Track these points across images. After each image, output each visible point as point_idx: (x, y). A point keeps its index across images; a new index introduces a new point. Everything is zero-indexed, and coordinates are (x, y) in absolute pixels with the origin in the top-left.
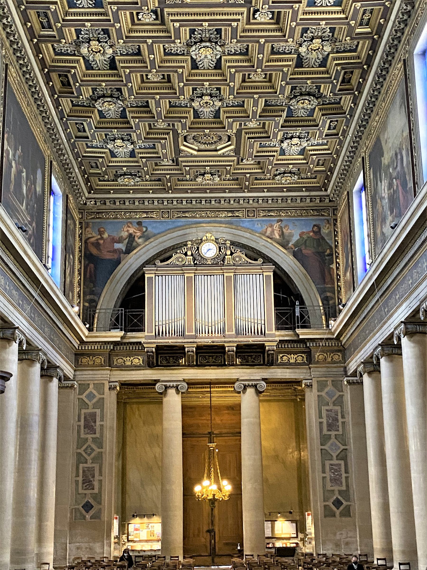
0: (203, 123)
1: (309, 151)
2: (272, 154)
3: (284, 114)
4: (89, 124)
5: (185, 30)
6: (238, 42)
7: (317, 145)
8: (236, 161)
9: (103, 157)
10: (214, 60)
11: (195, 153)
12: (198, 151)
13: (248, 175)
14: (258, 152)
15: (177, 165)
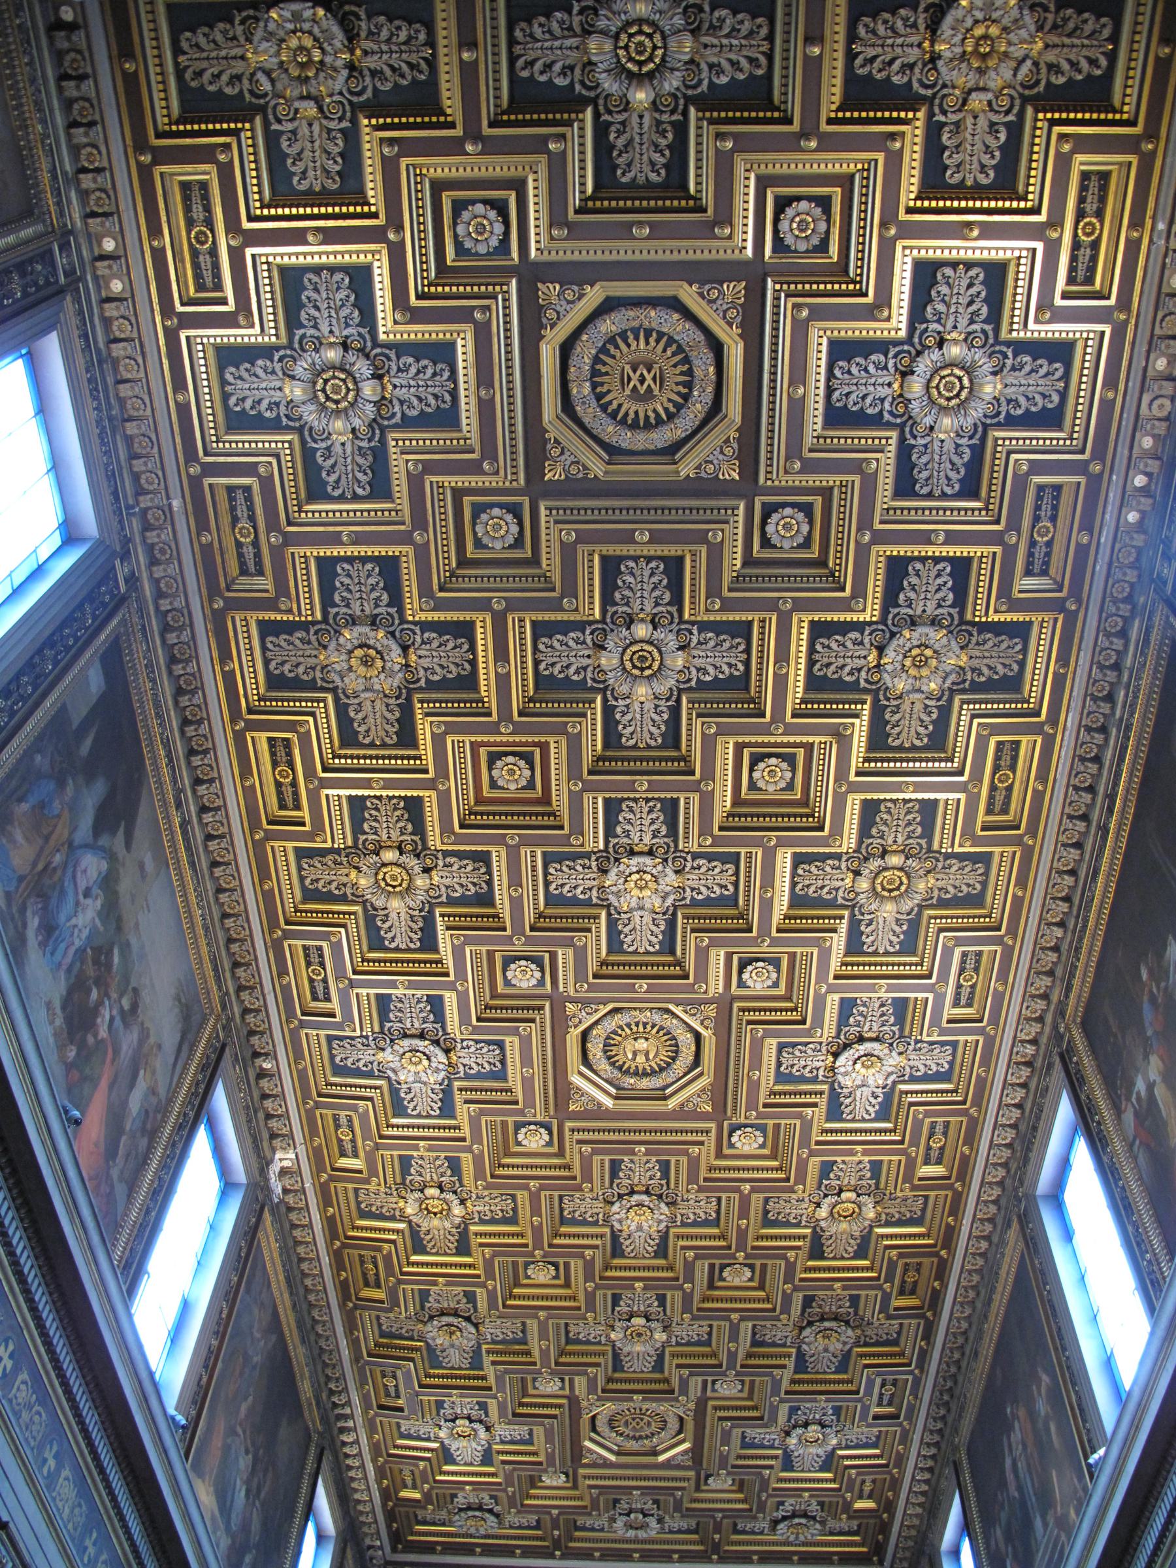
0: (629, 1381)
1: (907, 1093)
2: (808, 1100)
3: (844, 926)
4: (336, 948)
5: (605, 1295)
6: (701, 1189)
7: (926, 1079)
8: (713, 1134)
9: (371, 1099)
10: (655, 1235)
11: (609, 1103)
12: (616, 1098)
13: (747, 1187)
14: (773, 1093)
15: (561, 1154)
